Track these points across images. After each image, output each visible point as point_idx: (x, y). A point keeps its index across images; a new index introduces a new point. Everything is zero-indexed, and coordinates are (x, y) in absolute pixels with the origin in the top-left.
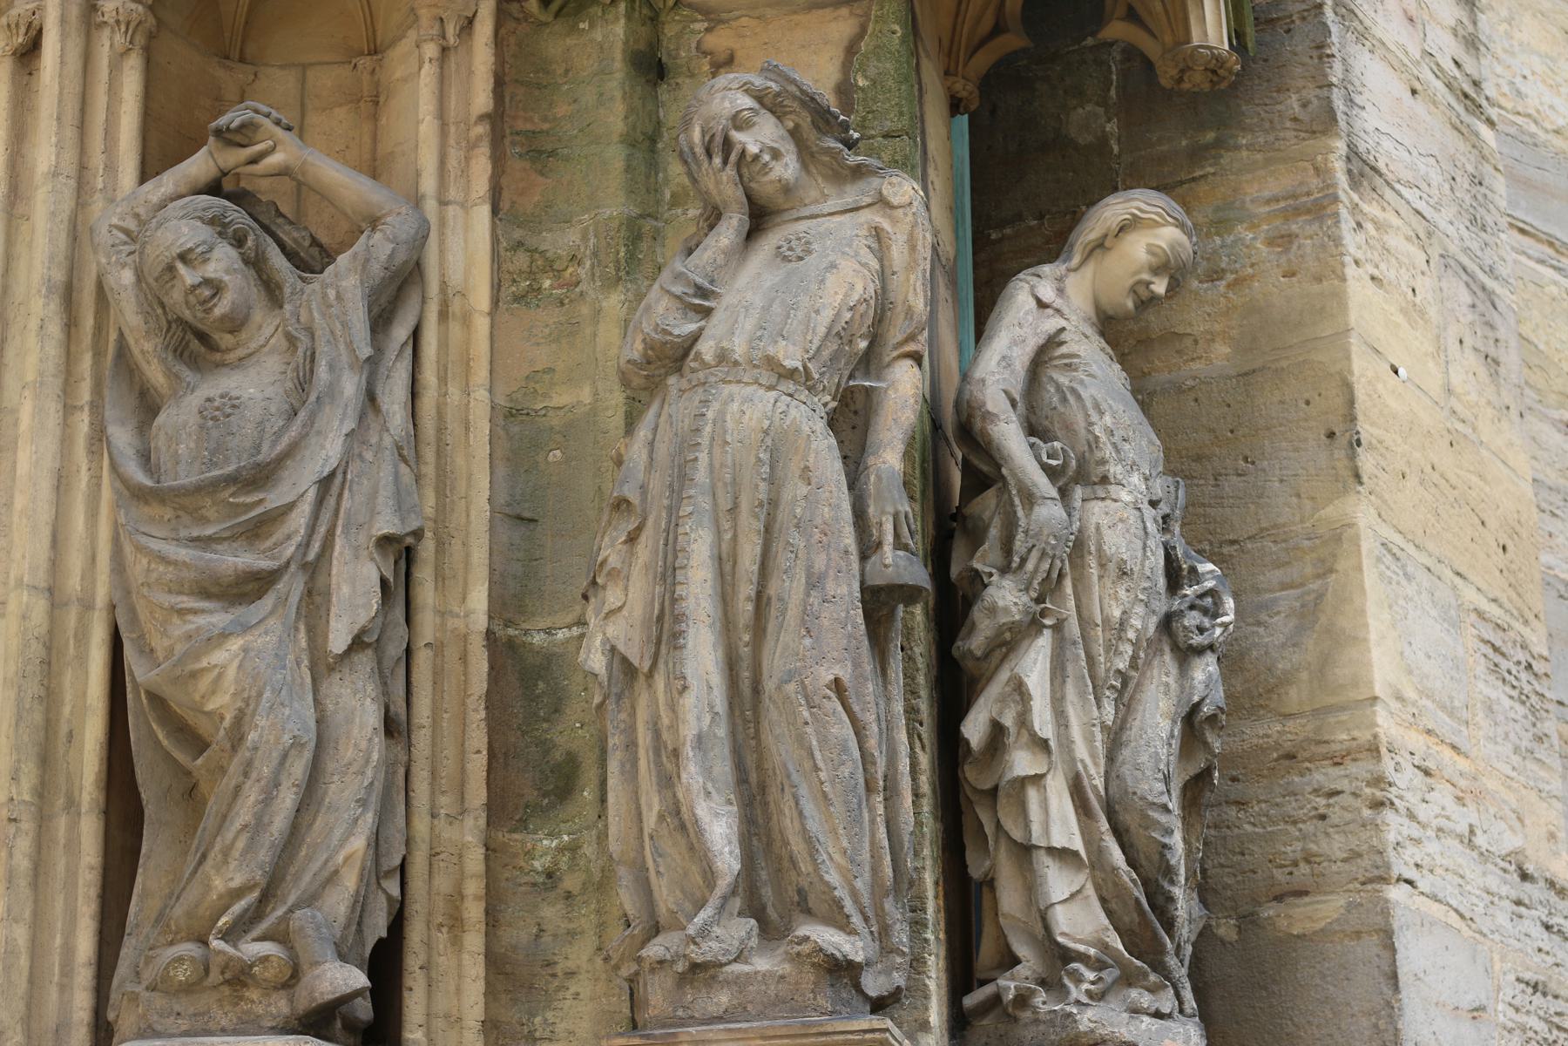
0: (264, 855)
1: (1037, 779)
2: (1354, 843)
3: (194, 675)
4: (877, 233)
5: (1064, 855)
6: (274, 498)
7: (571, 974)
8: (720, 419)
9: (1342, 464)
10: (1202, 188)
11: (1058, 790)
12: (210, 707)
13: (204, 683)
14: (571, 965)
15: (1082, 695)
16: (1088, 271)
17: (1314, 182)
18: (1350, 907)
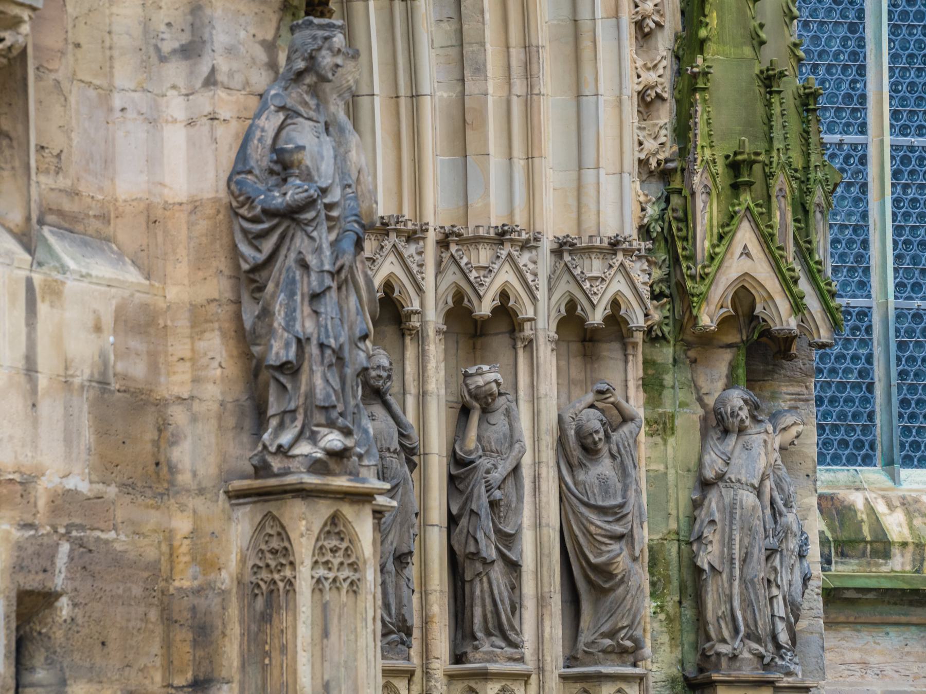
0: (631, 617)
1: (776, 596)
2: (811, 605)
3: (613, 564)
4: (765, 441)
5: (781, 618)
6: (625, 511)
7: (662, 644)
8: (741, 502)
9: (811, 486)
10: (767, 384)
11: (780, 597)
12: (615, 572)
13: (615, 566)
14: (662, 641)
15: (787, 572)
16: (780, 436)
17: (805, 391)
18: (810, 625)
